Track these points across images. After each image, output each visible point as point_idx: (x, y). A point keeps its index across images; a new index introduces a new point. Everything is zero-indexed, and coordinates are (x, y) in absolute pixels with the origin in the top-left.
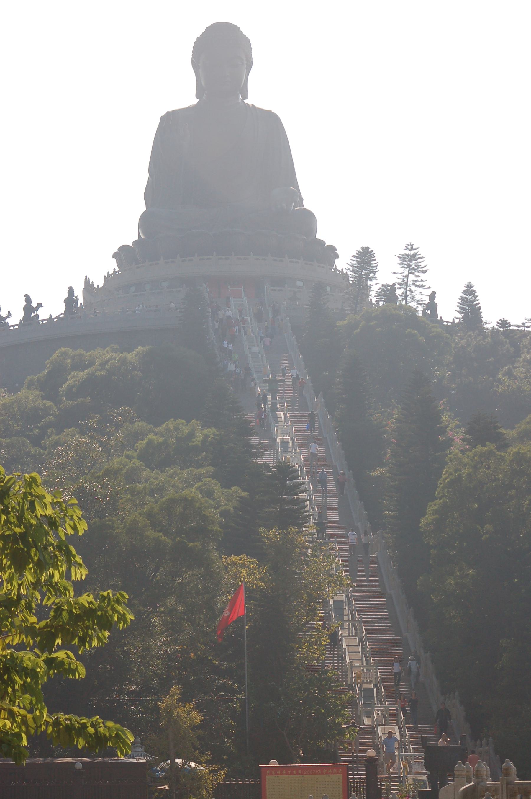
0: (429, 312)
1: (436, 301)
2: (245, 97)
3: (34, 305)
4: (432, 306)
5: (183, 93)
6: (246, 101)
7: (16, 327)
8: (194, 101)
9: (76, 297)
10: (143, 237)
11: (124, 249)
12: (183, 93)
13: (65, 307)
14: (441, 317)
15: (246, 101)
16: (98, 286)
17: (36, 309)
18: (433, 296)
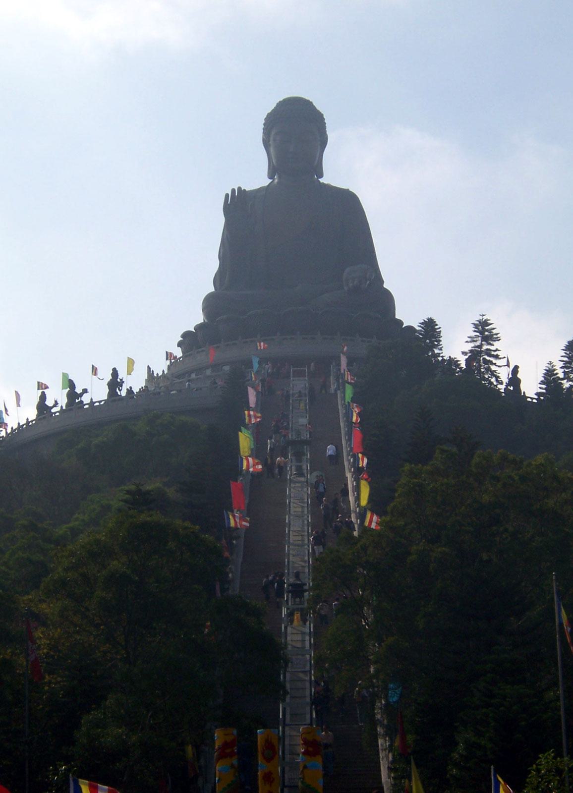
0: (512, 388)
1: (519, 376)
2: (321, 176)
3: (78, 390)
4: (515, 380)
5: (254, 173)
6: (321, 180)
7: (58, 414)
8: (266, 182)
9: (121, 380)
10: (206, 321)
11: (186, 335)
12: (254, 173)
13: (108, 390)
14: (524, 393)
15: (321, 180)
16: (157, 374)
17: (81, 395)
18: (516, 370)
